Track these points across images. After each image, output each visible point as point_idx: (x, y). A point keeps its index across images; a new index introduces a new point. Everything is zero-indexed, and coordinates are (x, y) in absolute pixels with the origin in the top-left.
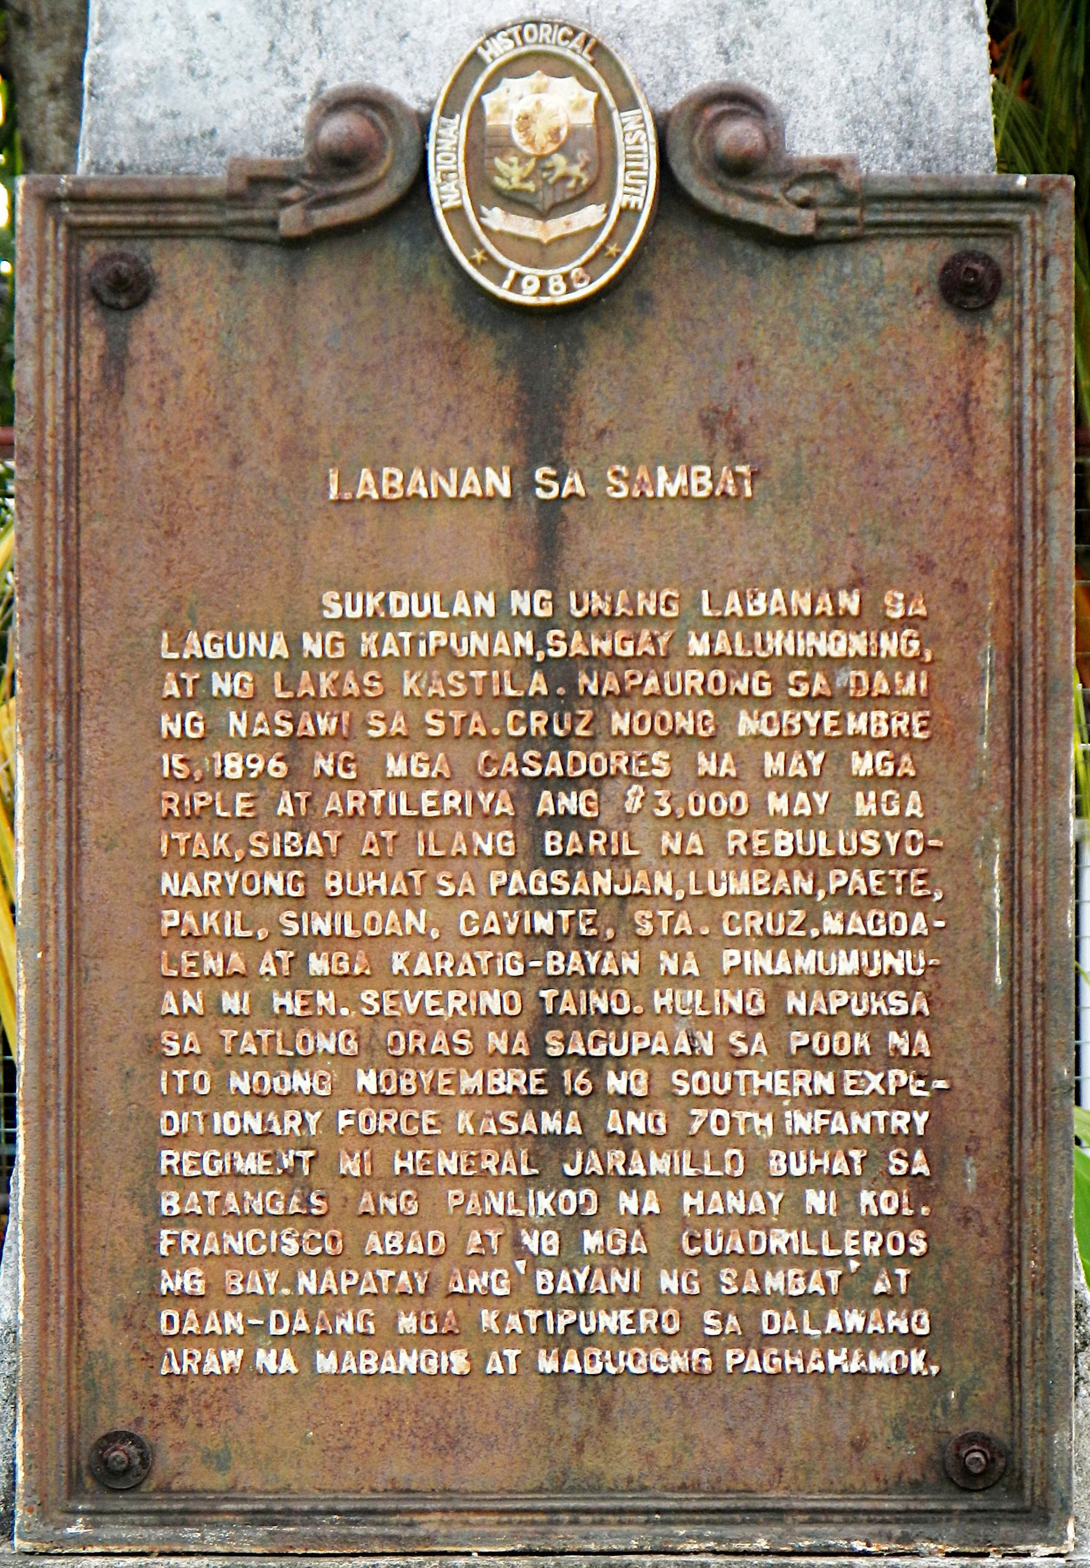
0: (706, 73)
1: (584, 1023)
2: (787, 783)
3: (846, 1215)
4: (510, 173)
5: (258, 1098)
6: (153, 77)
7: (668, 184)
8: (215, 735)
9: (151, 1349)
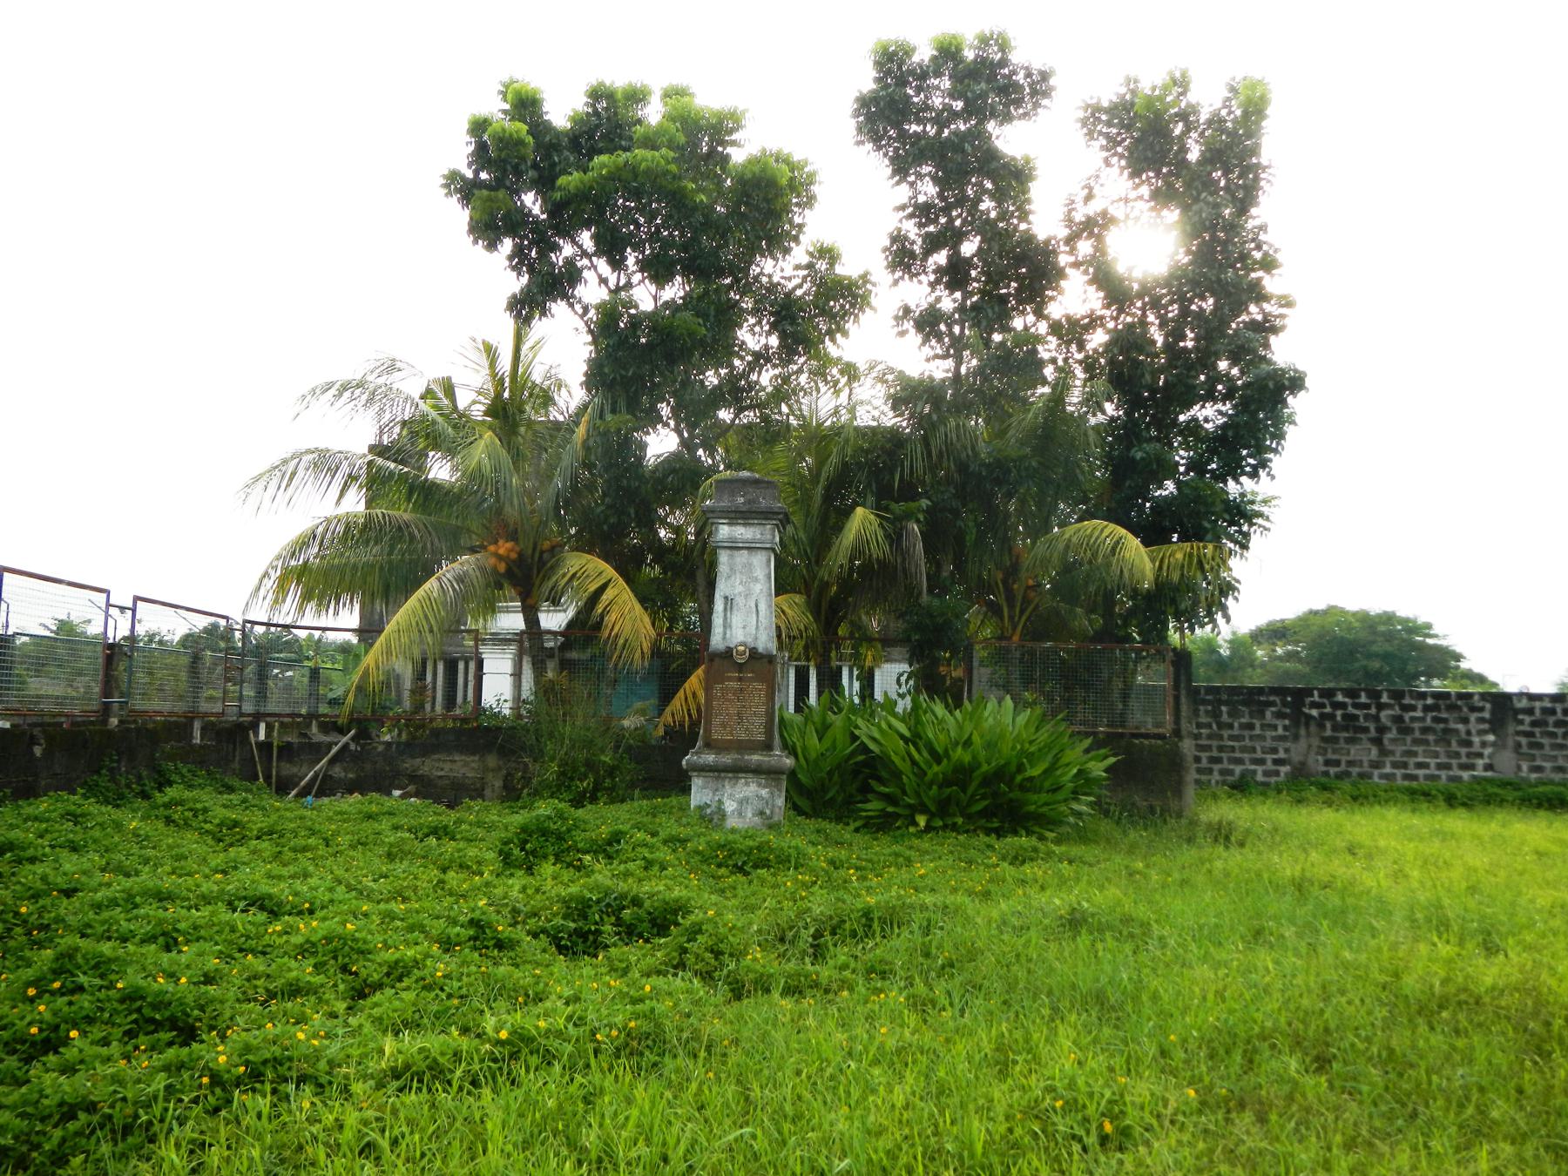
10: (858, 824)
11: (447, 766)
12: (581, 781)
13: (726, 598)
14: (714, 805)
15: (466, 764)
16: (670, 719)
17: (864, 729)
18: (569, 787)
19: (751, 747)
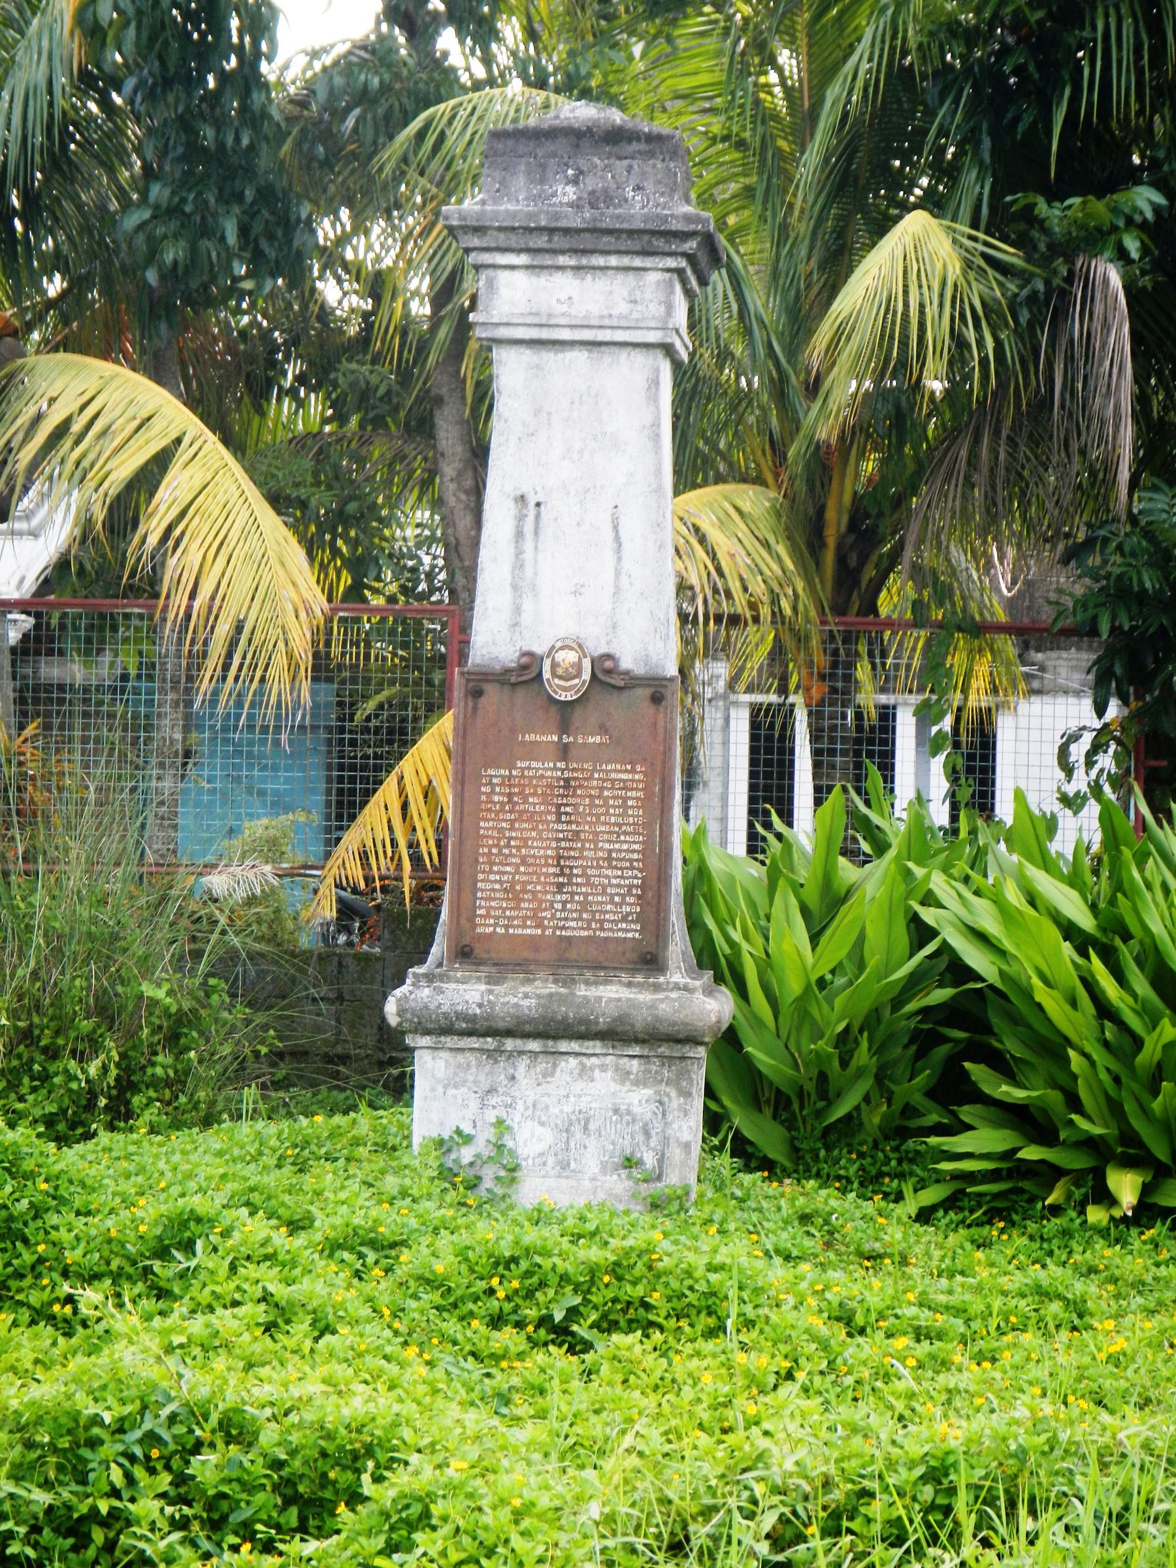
0: (603, 649)
3: (623, 903)
4: (560, 671)
7: (593, 675)
8: (493, 792)
9: (474, 926)
10: (932, 1195)
13: (522, 499)
14: (484, 1137)
16: (356, 872)
17: (954, 912)
18: (45, 1077)
19: (601, 961)
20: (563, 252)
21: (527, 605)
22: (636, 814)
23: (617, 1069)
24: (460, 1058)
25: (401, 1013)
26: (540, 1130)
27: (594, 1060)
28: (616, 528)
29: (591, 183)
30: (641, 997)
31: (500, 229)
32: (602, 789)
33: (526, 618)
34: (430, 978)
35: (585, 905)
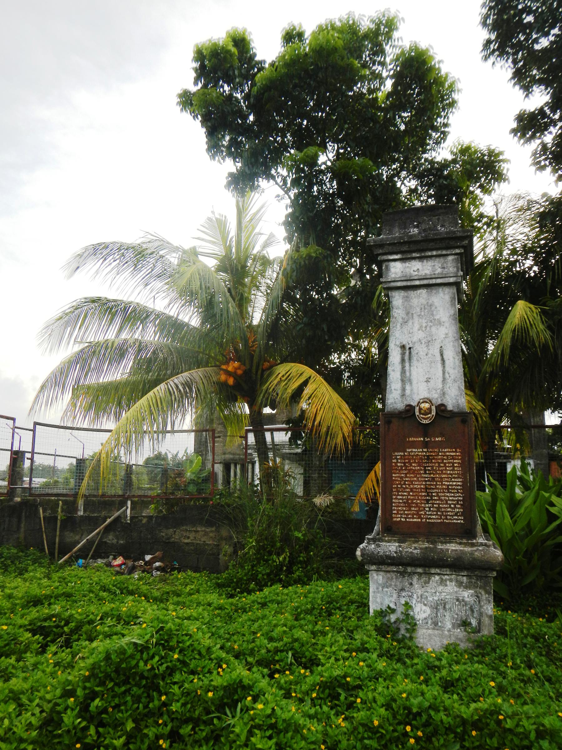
0: (439, 402)
1: (431, 489)
2: (449, 467)
3: (455, 507)
4: (422, 412)
5: (401, 495)
6: (392, 403)
8: (397, 462)
9: (393, 518)
11: (192, 535)
12: (278, 555)
13: (403, 347)
14: (400, 609)
15: (206, 534)
16: (364, 497)
18: (267, 561)
20: (414, 251)
21: (408, 387)
22: (458, 470)
23: (457, 581)
24: (389, 575)
25: (363, 555)
26: (424, 608)
27: (446, 577)
28: (442, 355)
29: (423, 226)
30: (466, 549)
31: (390, 244)
32: (443, 459)
33: (408, 392)
34: (374, 540)
35: (439, 509)
